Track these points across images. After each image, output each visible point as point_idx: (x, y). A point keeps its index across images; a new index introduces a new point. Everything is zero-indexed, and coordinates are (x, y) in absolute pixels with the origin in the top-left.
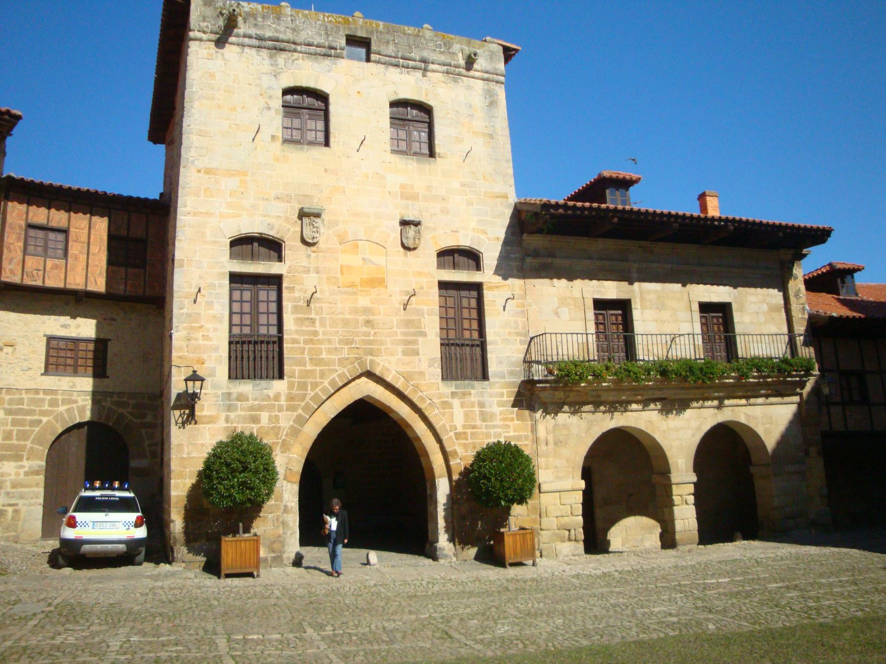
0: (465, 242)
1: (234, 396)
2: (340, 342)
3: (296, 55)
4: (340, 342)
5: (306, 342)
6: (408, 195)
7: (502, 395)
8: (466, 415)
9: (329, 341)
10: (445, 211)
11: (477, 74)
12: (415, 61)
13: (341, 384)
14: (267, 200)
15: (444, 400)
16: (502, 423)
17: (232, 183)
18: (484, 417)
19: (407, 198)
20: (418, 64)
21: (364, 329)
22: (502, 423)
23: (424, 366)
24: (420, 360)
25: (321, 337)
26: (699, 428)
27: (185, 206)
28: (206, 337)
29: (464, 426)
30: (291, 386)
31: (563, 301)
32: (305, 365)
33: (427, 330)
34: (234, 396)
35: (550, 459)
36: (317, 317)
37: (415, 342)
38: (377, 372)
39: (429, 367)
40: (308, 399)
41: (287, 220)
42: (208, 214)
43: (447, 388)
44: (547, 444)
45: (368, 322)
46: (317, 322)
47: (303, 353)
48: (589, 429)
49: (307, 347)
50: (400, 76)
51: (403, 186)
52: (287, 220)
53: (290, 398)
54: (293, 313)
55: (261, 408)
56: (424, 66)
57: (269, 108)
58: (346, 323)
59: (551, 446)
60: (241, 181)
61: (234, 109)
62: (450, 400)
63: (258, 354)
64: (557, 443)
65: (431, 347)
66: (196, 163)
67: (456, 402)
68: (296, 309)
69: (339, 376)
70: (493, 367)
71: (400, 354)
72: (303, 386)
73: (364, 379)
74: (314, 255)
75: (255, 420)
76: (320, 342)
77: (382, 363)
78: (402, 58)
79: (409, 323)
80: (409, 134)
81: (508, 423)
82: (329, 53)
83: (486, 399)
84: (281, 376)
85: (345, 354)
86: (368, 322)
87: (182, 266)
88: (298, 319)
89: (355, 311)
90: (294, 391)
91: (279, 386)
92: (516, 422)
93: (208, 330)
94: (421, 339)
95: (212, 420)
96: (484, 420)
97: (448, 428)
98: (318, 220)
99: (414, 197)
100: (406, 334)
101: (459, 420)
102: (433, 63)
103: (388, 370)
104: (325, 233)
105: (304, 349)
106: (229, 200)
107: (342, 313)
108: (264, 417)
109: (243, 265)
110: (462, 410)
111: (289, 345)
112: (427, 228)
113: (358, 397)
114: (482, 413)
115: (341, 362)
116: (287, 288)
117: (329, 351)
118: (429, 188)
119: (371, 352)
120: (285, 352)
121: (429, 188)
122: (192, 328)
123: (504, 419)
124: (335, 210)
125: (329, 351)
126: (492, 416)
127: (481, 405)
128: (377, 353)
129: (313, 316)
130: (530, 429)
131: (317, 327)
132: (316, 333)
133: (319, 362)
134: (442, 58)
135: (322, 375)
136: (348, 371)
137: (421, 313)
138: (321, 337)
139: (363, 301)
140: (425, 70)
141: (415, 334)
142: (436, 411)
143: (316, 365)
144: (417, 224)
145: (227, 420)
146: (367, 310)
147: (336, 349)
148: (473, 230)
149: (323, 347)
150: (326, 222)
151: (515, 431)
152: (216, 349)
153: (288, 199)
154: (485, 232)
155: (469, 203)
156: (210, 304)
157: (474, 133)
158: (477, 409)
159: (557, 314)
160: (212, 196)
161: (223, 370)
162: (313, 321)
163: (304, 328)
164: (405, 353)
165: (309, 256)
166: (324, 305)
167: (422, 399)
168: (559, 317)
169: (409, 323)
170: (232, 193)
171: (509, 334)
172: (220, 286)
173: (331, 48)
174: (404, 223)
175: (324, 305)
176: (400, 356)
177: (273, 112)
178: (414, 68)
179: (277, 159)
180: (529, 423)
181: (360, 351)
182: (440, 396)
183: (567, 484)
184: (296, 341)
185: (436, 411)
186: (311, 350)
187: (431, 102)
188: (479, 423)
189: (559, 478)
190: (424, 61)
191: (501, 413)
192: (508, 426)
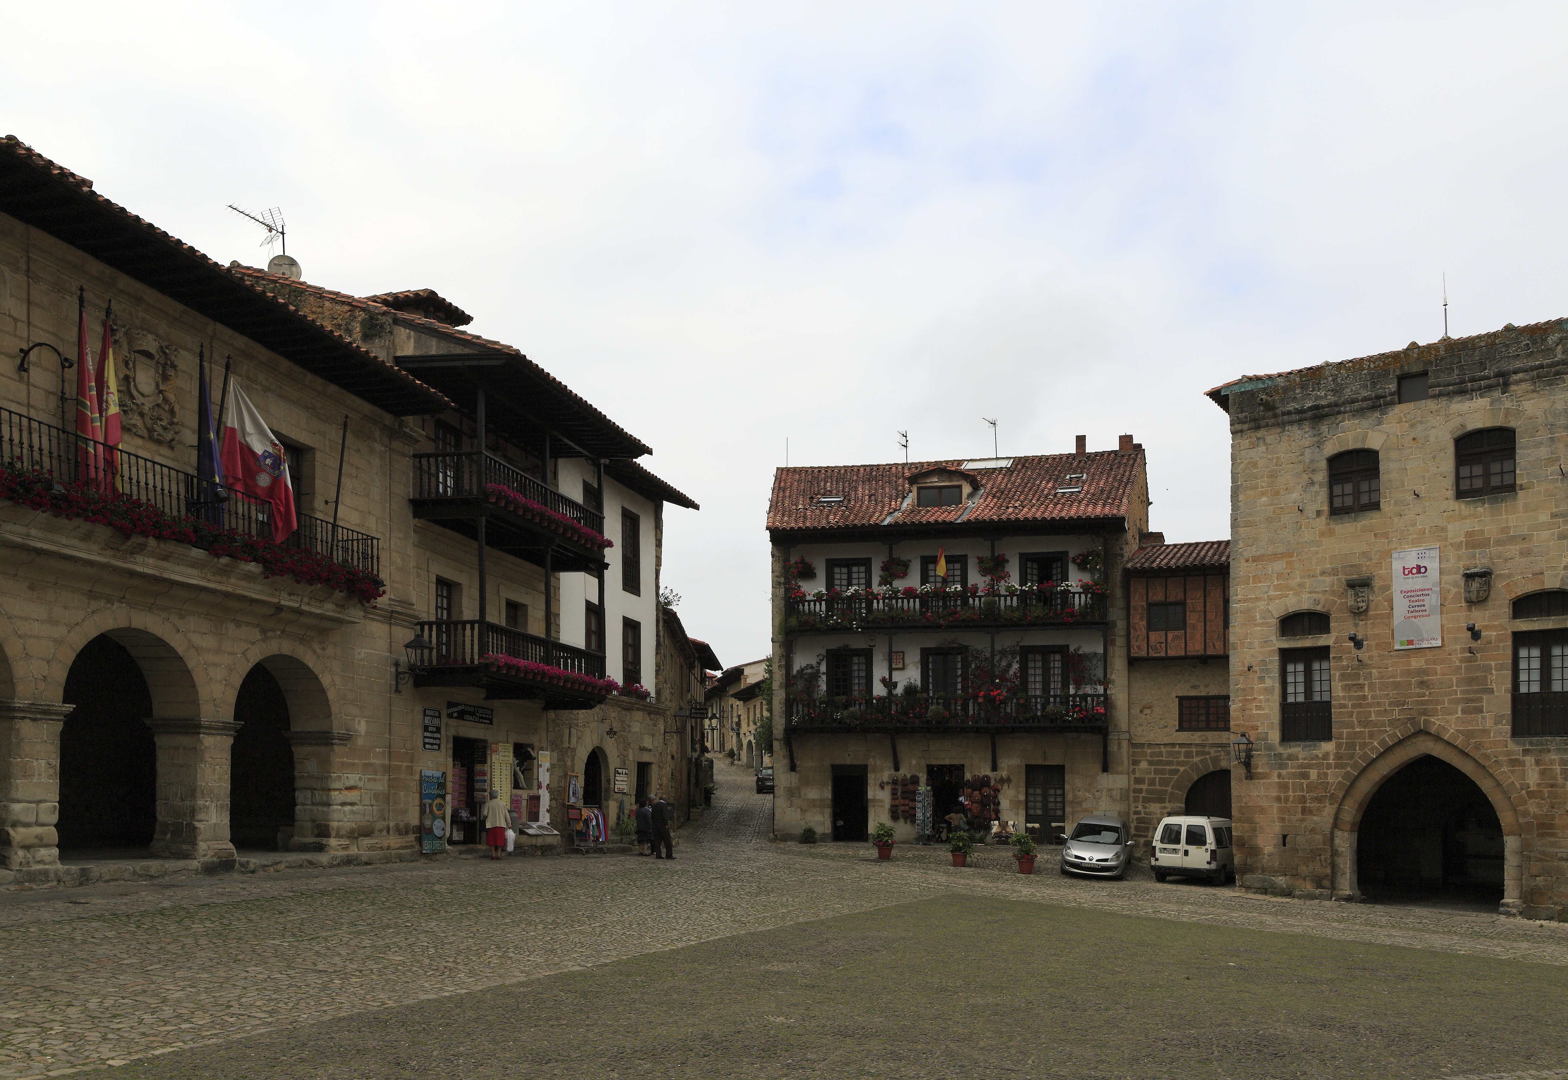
2: (1390, 704)
4: (1390, 704)
8: (1543, 773)
9: (1379, 704)
13: (1391, 744)
14: (1313, 576)
17: (1279, 566)
21: (1417, 690)
23: (1489, 723)
24: (1483, 718)
25: (1370, 700)
27: (1237, 595)
29: (1539, 785)
32: (1353, 727)
36: (1366, 682)
38: (1433, 730)
40: (1356, 758)
41: (1333, 593)
42: (1257, 599)
45: (1422, 684)
46: (1366, 686)
47: (1351, 716)
52: (1333, 593)
54: (1340, 680)
58: (1397, 685)
60: (1287, 563)
62: (1521, 758)
63: (1306, 721)
66: (1245, 553)
67: (1529, 760)
68: (1343, 677)
71: (1460, 712)
72: (1351, 746)
74: (1361, 623)
76: (1369, 705)
77: (1438, 723)
84: (1329, 738)
85: (1396, 715)
87: (1235, 649)
88: (1346, 685)
89: (1408, 673)
91: (1328, 747)
93: (1260, 701)
97: (1518, 786)
98: (1366, 589)
100: (1467, 692)
101: (1533, 778)
103: (1444, 728)
105: (1352, 712)
106: (1276, 583)
107: (1392, 677)
109: (1291, 642)
110: (1537, 768)
115: (1391, 723)
116: (1334, 658)
119: (1425, 713)
120: (1333, 716)
122: (1247, 700)
125: (1378, 713)
128: (1435, 713)
129: (1361, 682)
132: (1364, 697)
133: (1366, 723)
135: (1371, 736)
136: (1400, 731)
138: (1370, 700)
142: (1505, 769)
143: (1364, 727)
146: (1420, 672)
147: (1385, 710)
149: (1372, 710)
150: (1376, 589)
153: (1334, 572)
156: (1262, 679)
160: (1260, 582)
161: (1275, 736)
164: (1464, 711)
166: (1374, 671)
167: (1486, 756)
170: (1279, 576)
172: (1271, 662)
175: (1374, 671)
176: (1459, 714)
179: (1322, 534)
182: (1508, 753)
184: (1344, 706)
185: (1505, 769)
186: (1358, 713)
188: (1560, 781)
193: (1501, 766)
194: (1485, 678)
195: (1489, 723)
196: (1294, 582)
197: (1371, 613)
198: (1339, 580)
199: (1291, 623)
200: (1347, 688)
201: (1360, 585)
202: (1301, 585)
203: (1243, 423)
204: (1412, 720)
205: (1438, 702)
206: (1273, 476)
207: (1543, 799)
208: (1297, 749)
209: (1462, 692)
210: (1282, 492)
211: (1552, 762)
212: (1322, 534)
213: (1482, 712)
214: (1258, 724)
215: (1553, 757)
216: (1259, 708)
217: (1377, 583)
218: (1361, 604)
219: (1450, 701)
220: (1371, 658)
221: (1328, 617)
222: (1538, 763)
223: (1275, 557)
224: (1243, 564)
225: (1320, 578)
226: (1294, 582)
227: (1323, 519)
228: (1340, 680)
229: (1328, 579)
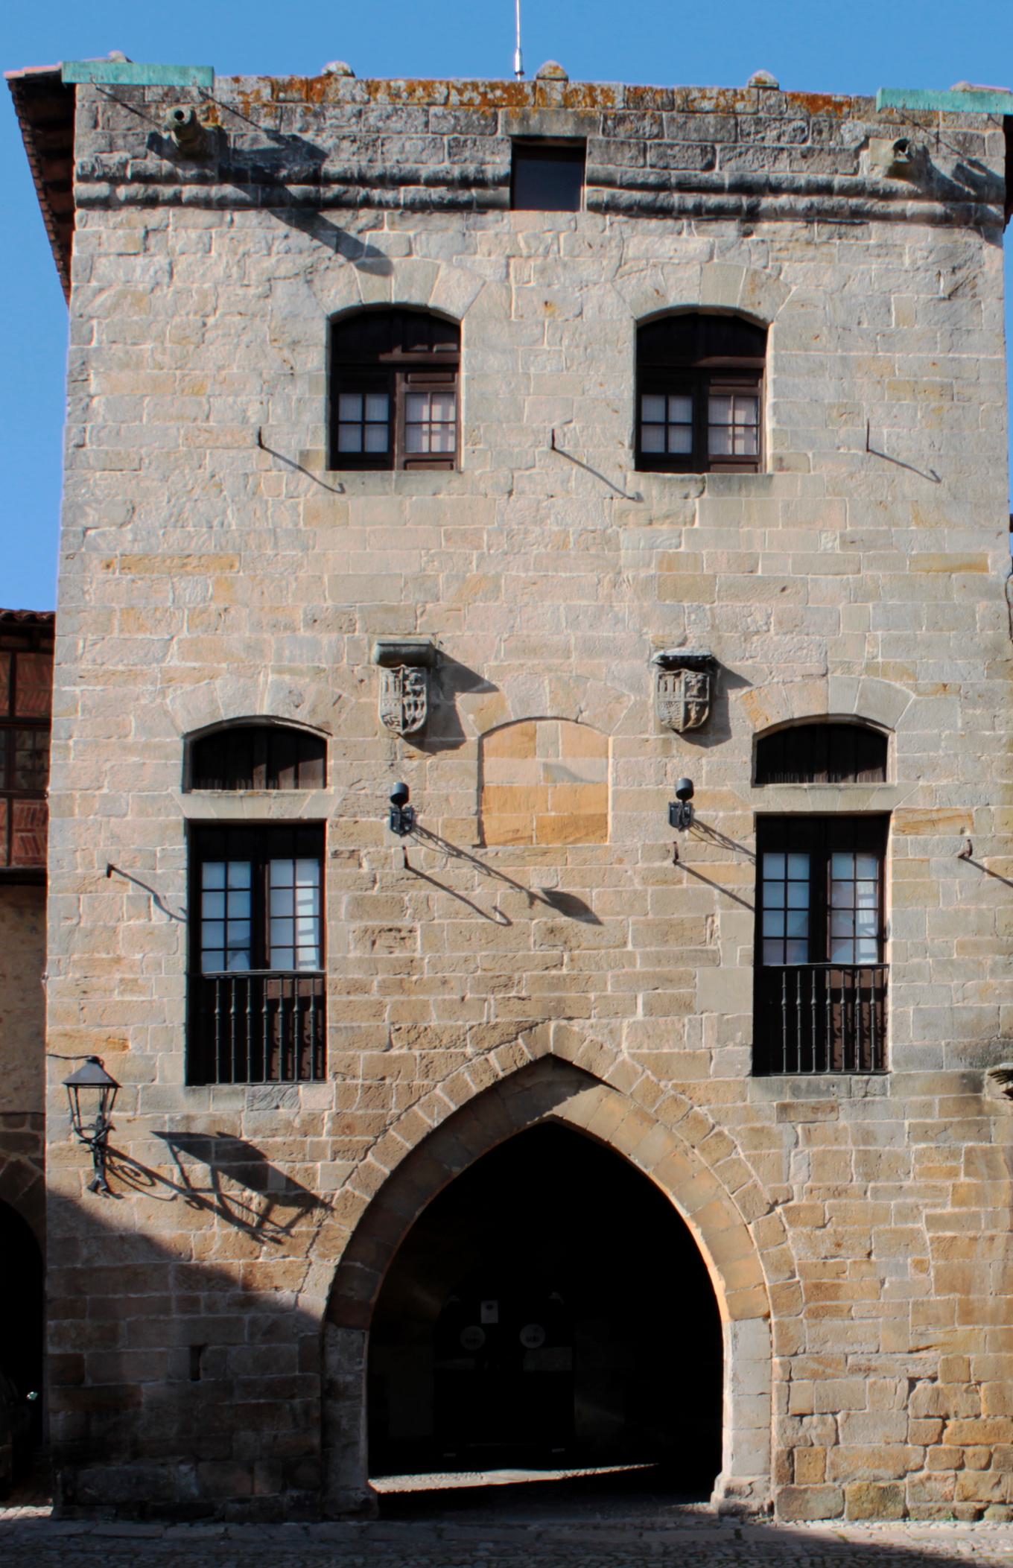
6: (676, 583)
8: (819, 1163)
15: (758, 1125)
16: (921, 1182)
22: (921, 1182)
47: (378, 1015)
49: (388, 999)
54: (352, 917)
68: (359, 906)
77: (590, 1035)
79: (665, 931)
96: (868, 1176)
111: (337, 998)
114: (865, 1158)
123: (928, 1173)
127: (866, 1136)
129: (405, 923)
141: (679, 958)
149: (431, 998)
151: (956, 1203)
158: (851, 1147)
164: (649, 1010)
169: (665, 931)
181: (528, 1006)
191: (921, 1156)
198: (355, 644)
199: (228, 752)
202: (254, 649)
209: (647, 958)
212: (313, 516)
218: (410, 714)
228: (352, 917)
229: (327, 639)
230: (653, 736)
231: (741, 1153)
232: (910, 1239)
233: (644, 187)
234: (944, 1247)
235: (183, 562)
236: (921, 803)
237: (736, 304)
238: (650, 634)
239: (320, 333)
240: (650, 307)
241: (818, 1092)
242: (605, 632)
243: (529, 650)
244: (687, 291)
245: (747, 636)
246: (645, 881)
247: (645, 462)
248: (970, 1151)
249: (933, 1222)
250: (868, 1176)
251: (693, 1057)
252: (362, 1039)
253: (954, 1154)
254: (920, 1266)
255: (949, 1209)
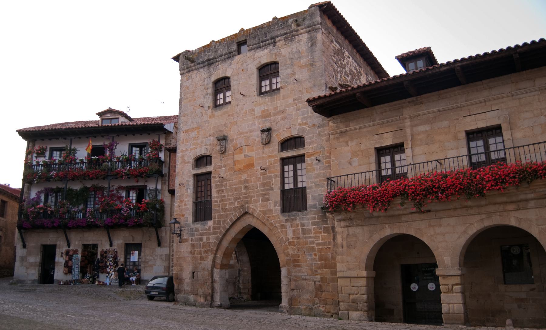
0: (295, 133)
1: (194, 229)
3: (217, 63)
5: (220, 201)
7: (315, 218)
8: (294, 232)
9: (229, 199)
10: (284, 119)
11: (302, 31)
12: (268, 40)
16: (314, 235)
17: (194, 134)
18: (304, 232)
19: (265, 118)
20: (270, 41)
22: (314, 235)
25: (226, 198)
26: (465, 232)
28: (185, 205)
29: (293, 238)
30: (214, 223)
31: (354, 154)
33: (273, 186)
34: (194, 229)
35: (344, 257)
37: (268, 194)
38: (250, 212)
39: (274, 206)
43: (282, 218)
44: (342, 247)
48: (371, 236)
50: (262, 52)
51: (263, 112)
53: (214, 228)
54: (215, 188)
55: (202, 234)
56: (273, 41)
57: (207, 94)
58: (236, 189)
59: (345, 248)
61: (195, 100)
62: (284, 223)
63: (202, 210)
64: (348, 247)
65: (276, 196)
68: (217, 186)
69: (234, 216)
70: (310, 202)
72: (219, 222)
73: (247, 216)
74: (223, 158)
75: (201, 239)
77: (252, 207)
78: (262, 42)
80: (271, 82)
81: (318, 235)
82: (230, 56)
83: (305, 222)
84: (210, 219)
85: (236, 205)
86: (246, 187)
89: (240, 182)
90: (216, 225)
91: (210, 223)
92: (323, 234)
94: (270, 192)
95: (186, 240)
96: (304, 234)
99: (268, 116)
101: (290, 235)
102: (278, 37)
103: (255, 210)
104: (230, 146)
108: (205, 238)
112: (274, 130)
113: (244, 225)
115: (235, 209)
117: (230, 204)
118: (276, 108)
119: (247, 202)
121: (276, 108)
123: (316, 233)
124: (232, 134)
125: (230, 204)
126: (309, 231)
127: (303, 225)
129: (223, 188)
130: (332, 238)
131: (225, 194)
132: (224, 196)
133: (225, 210)
134: (283, 31)
137: (270, 177)
138: (226, 198)
139: (244, 177)
140: (275, 43)
142: (279, 230)
144: (269, 130)
145: (192, 240)
146: (246, 181)
148: (300, 124)
151: (322, 240)
152: (188, 209)
154: (306, 124)
155: (298, 110)
157: (301, 67)
159: (350, 163)
161: (190, 219)
162: (223, 191)
163: (220, 195)
164: (262, 201)
165: (221, 160)
168: (351, 165)
169: (264, 185)
171: (320, 181)
173: (230, 53)
174: (263, 131)
177: (209, 95)
178: (269, 44)
179: (210, 117)
180: (332, 234)
182: (280, 222)
183: (354, 273)
184: (216, 202)
187: (277, 60)
188: (301, 235)
189: (349, 269)
190: (273, 38)
191: (314, 229)
192: (318, 237)
193: (278, 229)
194: (270, 182)
195: (272, 205)
196: (199, 141)
197: (227, 153)
200: (218, 192)
201: (223, 139)
202: (202, 142)
203: (184, 70)
204: (242, 207)
205: (252, 197)
206: (194, 92)
207: (295, 246)
208: (198, 226)
210: (197, 99)
211: (297, 226)
213: (269, 200)
214: (184, 213)
215: (298, 222)
216: (185, 205)
217: (230, 138)
219: (257, 196)
220: (227, 176)
221: (211, 156)
222: (292, 227)
223: (193, 130)
224: (182, 134)
225: (209, 138)
226: (199, 141)
227: (210, 110)
228: (215, 188)
229: (212, 138)
230: (261, 146)
231: (279, 230)
232: (313, 249)
233: (256, 44)
234: (320, 250)
235: (193, 130)
236: (311, 151)
237: (273, 60)
238: (260, 126)
239: (211, 85)
240: (259, 65)
241: (293, 216)
242: (253, 128)
243: (241, 134)
244: (264, 61)
245: (277, 123)
246: (261, 175)
247: (261, 93)
248: (324, 227)
249: (318, 244)
250: (304, 234)
251: (270, 210)
252: (218, 211)
253: (321, 228)
254: (315, 255)
255: (320, 241)
